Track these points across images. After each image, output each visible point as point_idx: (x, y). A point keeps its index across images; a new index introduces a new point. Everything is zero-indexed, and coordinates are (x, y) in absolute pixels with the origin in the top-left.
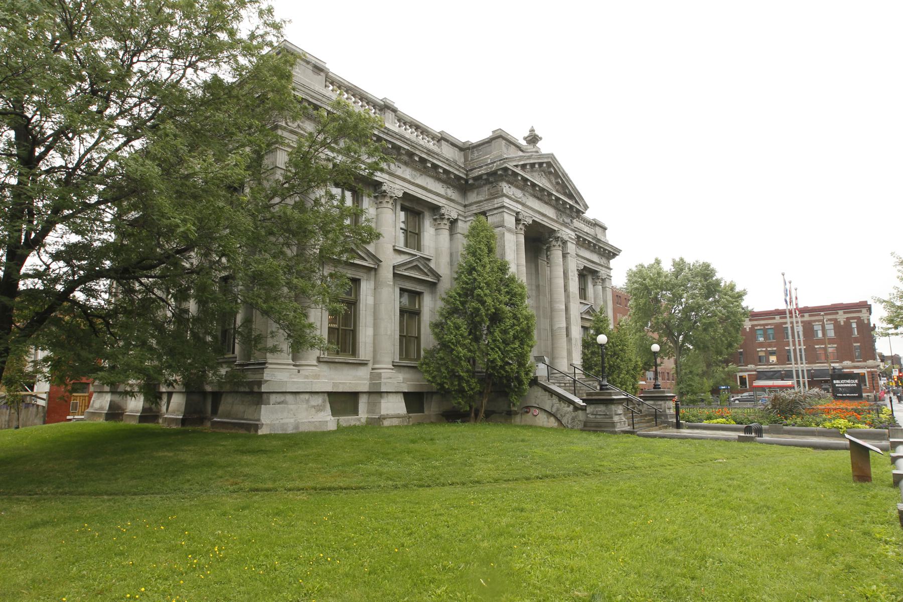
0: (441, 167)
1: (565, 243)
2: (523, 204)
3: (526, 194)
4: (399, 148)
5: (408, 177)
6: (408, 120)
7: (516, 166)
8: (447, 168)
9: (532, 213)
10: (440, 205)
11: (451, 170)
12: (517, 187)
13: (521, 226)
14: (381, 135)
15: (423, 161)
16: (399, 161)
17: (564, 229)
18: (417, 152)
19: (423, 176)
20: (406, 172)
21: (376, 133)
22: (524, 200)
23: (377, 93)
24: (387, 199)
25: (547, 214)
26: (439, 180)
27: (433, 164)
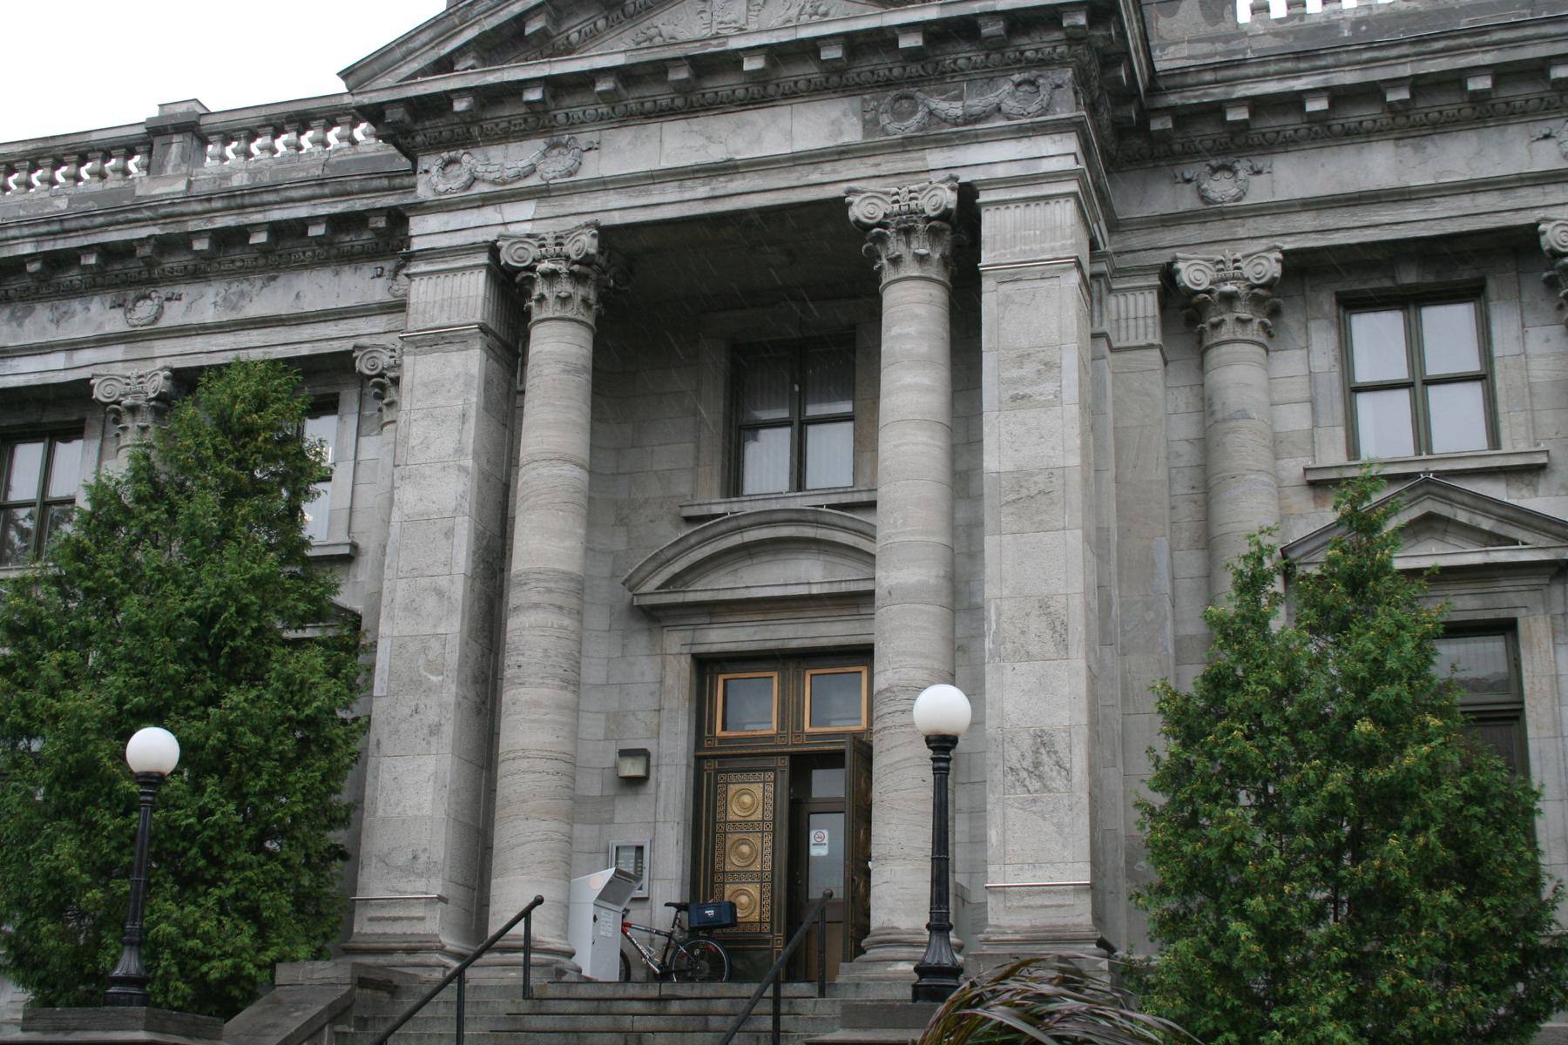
0: (314, 220)
1: (960, 228)
2: (542, 193)
3: (585, 137)
4: (124, 251)
5: (210, 316)
6: (252, 119)
7: (444, 66)
8: (340, 208)
9: (614, 200)
10: (347, 345)
11: (359, 204)
12: (506, 136)
13: (540, 288)
14: (48, 247)
16: (171, 279)
17: (936, 158)
18: (193, 225)
19: (282, 280)
20: (204, 303)
21: (28, 249)
22: (554, 168)
23: (127, 107)
24: (127, 421)
25: (785, 149)
26: (352, 258)
27: (276, 229)
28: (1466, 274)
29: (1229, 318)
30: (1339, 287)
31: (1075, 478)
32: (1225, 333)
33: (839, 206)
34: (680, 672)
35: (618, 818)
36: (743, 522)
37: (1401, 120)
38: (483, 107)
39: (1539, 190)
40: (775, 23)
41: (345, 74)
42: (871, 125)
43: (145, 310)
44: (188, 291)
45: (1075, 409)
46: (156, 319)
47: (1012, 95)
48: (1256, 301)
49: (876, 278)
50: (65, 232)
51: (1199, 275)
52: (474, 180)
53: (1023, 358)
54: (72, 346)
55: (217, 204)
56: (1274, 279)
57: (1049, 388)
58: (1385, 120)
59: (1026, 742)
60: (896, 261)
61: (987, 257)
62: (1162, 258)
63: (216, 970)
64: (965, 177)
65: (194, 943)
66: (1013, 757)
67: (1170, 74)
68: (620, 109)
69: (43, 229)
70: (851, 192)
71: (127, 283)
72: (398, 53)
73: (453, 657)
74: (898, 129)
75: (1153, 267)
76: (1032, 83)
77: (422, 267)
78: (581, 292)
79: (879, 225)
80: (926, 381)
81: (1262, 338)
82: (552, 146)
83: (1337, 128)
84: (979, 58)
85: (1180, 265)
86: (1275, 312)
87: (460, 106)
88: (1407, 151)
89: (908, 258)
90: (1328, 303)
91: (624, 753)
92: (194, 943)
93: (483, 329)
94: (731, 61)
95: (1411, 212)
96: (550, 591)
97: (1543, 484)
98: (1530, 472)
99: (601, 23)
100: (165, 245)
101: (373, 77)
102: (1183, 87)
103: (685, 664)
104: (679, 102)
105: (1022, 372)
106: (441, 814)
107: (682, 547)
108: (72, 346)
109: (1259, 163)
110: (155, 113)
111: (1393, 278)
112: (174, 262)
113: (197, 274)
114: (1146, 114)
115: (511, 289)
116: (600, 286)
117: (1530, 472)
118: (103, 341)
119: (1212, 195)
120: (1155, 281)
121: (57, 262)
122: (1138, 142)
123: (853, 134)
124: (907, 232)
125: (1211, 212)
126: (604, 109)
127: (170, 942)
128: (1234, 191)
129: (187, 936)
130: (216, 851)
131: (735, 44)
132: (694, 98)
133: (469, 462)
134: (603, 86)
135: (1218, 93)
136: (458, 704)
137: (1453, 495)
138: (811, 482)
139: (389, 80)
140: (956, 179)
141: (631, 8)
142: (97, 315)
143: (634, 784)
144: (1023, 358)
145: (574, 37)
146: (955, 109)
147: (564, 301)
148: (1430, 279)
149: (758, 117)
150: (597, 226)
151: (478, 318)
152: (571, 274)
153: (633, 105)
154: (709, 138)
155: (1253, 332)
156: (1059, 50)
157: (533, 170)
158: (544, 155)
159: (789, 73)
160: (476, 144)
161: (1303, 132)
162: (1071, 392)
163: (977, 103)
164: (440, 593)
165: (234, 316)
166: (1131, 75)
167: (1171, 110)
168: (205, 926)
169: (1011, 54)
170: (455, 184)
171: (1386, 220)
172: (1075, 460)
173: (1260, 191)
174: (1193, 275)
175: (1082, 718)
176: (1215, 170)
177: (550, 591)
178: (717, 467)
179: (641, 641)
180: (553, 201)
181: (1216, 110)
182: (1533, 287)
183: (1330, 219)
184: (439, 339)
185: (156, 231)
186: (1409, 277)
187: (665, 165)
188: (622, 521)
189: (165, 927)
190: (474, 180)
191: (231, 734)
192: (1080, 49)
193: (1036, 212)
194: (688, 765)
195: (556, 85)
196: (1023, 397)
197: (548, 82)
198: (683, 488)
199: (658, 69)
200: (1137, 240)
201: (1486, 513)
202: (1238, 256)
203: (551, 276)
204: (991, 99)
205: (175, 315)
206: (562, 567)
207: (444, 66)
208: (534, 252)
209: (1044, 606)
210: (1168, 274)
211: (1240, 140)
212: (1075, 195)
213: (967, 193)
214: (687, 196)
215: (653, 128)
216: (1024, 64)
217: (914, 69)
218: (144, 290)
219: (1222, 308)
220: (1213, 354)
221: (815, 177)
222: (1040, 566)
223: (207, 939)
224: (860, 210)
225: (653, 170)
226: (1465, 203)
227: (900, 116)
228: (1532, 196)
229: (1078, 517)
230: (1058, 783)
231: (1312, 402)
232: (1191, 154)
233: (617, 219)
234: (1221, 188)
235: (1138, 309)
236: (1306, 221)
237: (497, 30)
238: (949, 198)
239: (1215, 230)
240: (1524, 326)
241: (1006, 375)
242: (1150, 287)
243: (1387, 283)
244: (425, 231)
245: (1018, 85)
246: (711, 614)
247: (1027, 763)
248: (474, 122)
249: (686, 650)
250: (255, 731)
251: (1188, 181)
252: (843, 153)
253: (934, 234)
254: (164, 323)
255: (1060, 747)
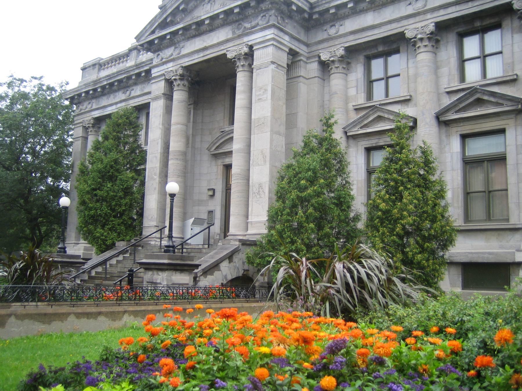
2: (173, 60)
3: (182, 44)
5: (138, 93)
7: (153, 32)
9: (186, 60)
12: (168, 47)
14: (109, 82)
15: (138, 75)
18: (132, 73)
21: (105, 83)
28: (395, 46)
29: (333, 67)
30: (365, 54)
31: (269, 119)
32: (332, 72)
33: (225, 55)
34: (221, 168)
35: (209, 205)
36: (229, 132)
37: (373, 5)
38: (162, 41)
39: (407, 20)
40: (217, 8)
41: (135, 38)
42: (234, 33)
43: (128, 93)
44: (134, 88)
45: (270, 101)
46: (130, 95)
47: (261, 20)
48: (340, 61)
49: (236, 70)
50: (111, 78)
51: (326, 56)
52: (162, 59)
53: (261, 88)
54: (116, 103)
55: (135, 68)
56: (342, 55)
57: (265, 96)
58: (369, 6)
59: (257, 186)
60: (238, 66)
61: (255, 63)
62: (316, 53)
63: (109, 242)
64: (250, 43)
65: (104, 237)
66: (255, 189)
67: (315, 3)
68: (186, 37)
69: (107, 78)
70: (227, 51)
71: (124, 88)
72: (144, 31)
73: (158, 172)
74: (238, 32)
75: (316, 55)
76: (265, 16)
77: (154, 81)
78: (182, 82)
79: (234, 58)
80: (243, 97)
81: (345, 71)
82: (175, 48)
83: (358, 10)
84: (253, 11)
85: (321, 55)
86: (349, 63)
87: (156, 42)
88: (376, 14)
89: (240, 66)
90: (362, 58)
91: (209, 190)
92: (104, 237)
93: (163, 94)
94: (203, 21)
95: (376, 31)
96: (175, 155)
97: (411, 104)
98: (406, 101)
99: (183, 16)
100: (129, 78)
101: (141, 37)
102: (319, 6)
103: (222, 167)
104: (197, 33)
105: (260, 93)
106: (156, 208)
107: (218, 139)
108: (116, 103)
109: (341, 23)
110: (130, 46)
111: (377, 49)
112: (131, 82)
113: (135, 84)
114: (311, 15)
115: (170, 83)
116: (187, 80)
117: (406, 101)
118: (121, 102)
119: (330, 34)
120: (317, 59)
121: (111, 85)
122: (312, 22)
123: (230, 36)
124: (239, 59)
125: (330, 39)
126: (183, 38)
127: (98, 237)
128: (335, 32)
129: (103, 236)
130: (106, 218)
131: (203, 18)
132: (200, 32)
133: (161, 126)
134: (180, 32)
135: (327, 6)
136: (160, 183)
137: (383, 110)
138: (391, 95)
139: (143, 38)
140: (248, 45)
141: (188, 11)
142: (121, 96)
143: (212, 196)
144: (261, 88)
145: (179, 20)
146: (248, 25)
147: (178, 85)
148: (386, 49)
149: (212, 34)
150: (182, 67)
151: (163, 92)
152: (179, 79)
153: (188, 35)
154: (204, 41)
155: (340, 70)
156: (270, 6)
157: (172, 55)
158: (174, 50)
159: (214, 23)
160: (163, 50)
161: (350, 13)
162: (269, 97)
163: (253, 23)
164: (156, 157)
165: (142, 93)
166: (298, 6)
167: (316, 12)
168: (105, 234)
169: (260, 9)
170: (159, 60)
171: (370, 34)
172: (269, 114)
173: (343, 30)
174: (324, 57)
175: (268, 180)
176: (331, 26)
177: (175, 155)
178: (228, 119)
179: (214, 163)
180: (176, 62)
181: (328, 10)
182: (410, 47)
183: (357, 36)
184: (156, 98)
185: (126, 75)
186: (381, 49)
187: (196, 49)
188: (210, 134)
189: (98, 235)
190: (162, 59)
191: (108, 193)
192: (274, 5)
193: (265, 50)
194: (222, 192)
195: (174, 34)
196: (260, 99)
197: (170, 33)
198: (222, 124)
199: (190, 25)
200: (314, 48)
201: (391, 114)
202: (335, 49)
203: (175, 79)
204: (256, 22)
205: (133, 94)
206: (177, 149)
207: (153, 32)
208: (172, 74)
209: (262, 152)
210: (319, 57)
211: (336, 17)
212: (273, 44)
213: (251, 47)
214: (199, 56)
215: (194, 40)
216: (262, 11)
217: (241, 17)
218: (127, 89)
219: (332, 64)
220: (331, 76)
221: (223, 48)
222: (263, 143)
223: (106, 237)
224: (229, 56)
225: (194, 51)
226: (389, 27)
227: (239, 29)
228: (405, 22)
229: (269, 129)
230: (263, 196)
231: (357, 87)
232: (325, 23)
233: (187, 64)
234: (332, 31)
235: (314, 67)
236: (352, 37)
237: (162, 22)
238: (246, 50)
239: (331, 43)
240: (408, 59)
241: (257, 94)
242: (316, 61)
243: (376, 51)
244: (155, 72)
245: (262, 17)
246: (226, 155)
247: (257, 191)
248: (161, 44)
249: (222, 164)
250: (114, 191)
251: (326, 30)
252: (227, 41)
253: (245, 59)
254: (131, 96)
255: (263, 187)
